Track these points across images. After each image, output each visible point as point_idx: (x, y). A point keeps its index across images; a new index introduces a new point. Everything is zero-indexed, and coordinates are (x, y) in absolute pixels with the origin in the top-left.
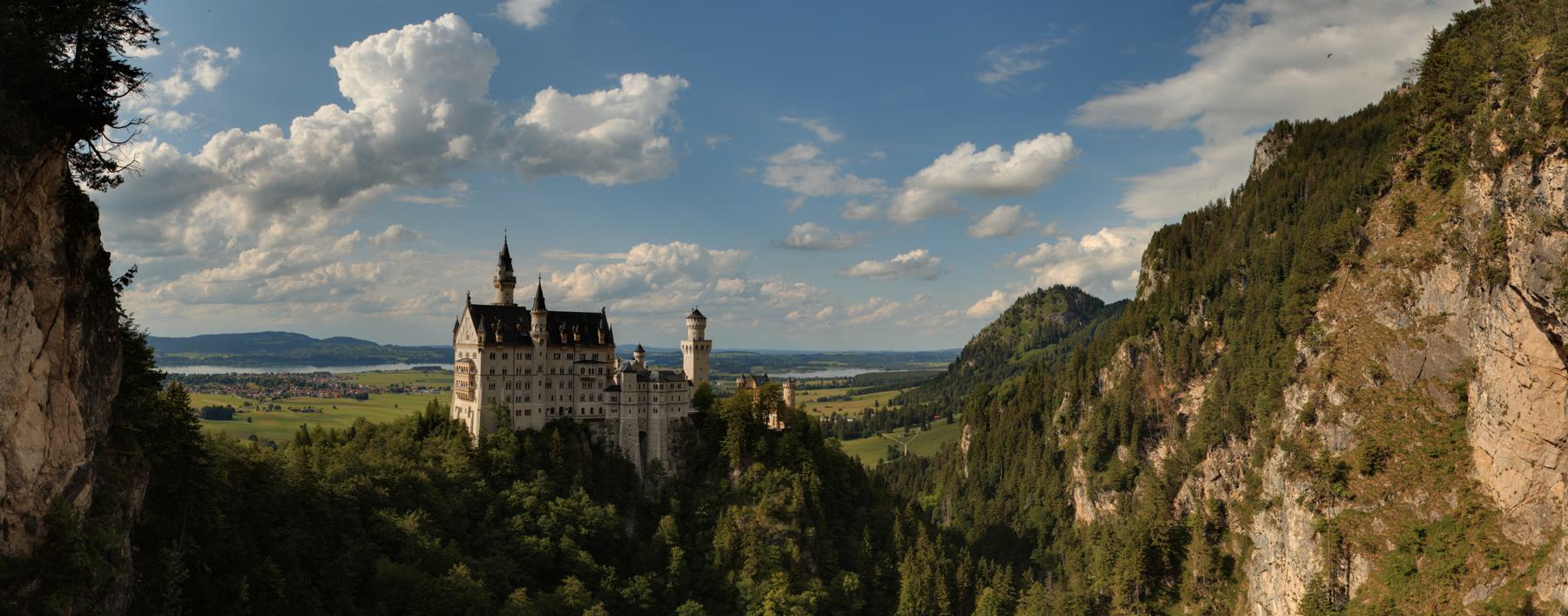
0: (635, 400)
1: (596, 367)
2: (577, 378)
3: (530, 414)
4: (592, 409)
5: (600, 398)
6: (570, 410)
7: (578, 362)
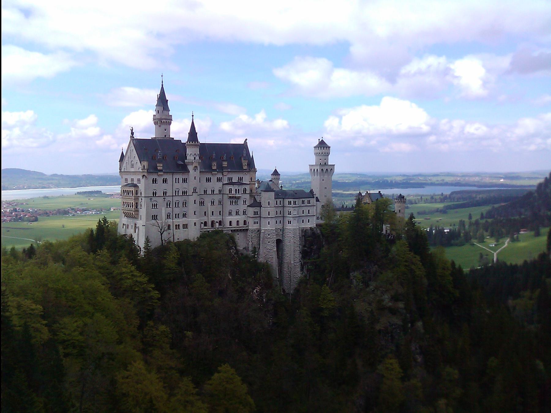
0: (273, 214)
1: (241, 188)
2: (226, 197)
3: (187, 228)
4: (238, 221)
5: (244, 213)
6: (220, 224)
7: (224, 184)
